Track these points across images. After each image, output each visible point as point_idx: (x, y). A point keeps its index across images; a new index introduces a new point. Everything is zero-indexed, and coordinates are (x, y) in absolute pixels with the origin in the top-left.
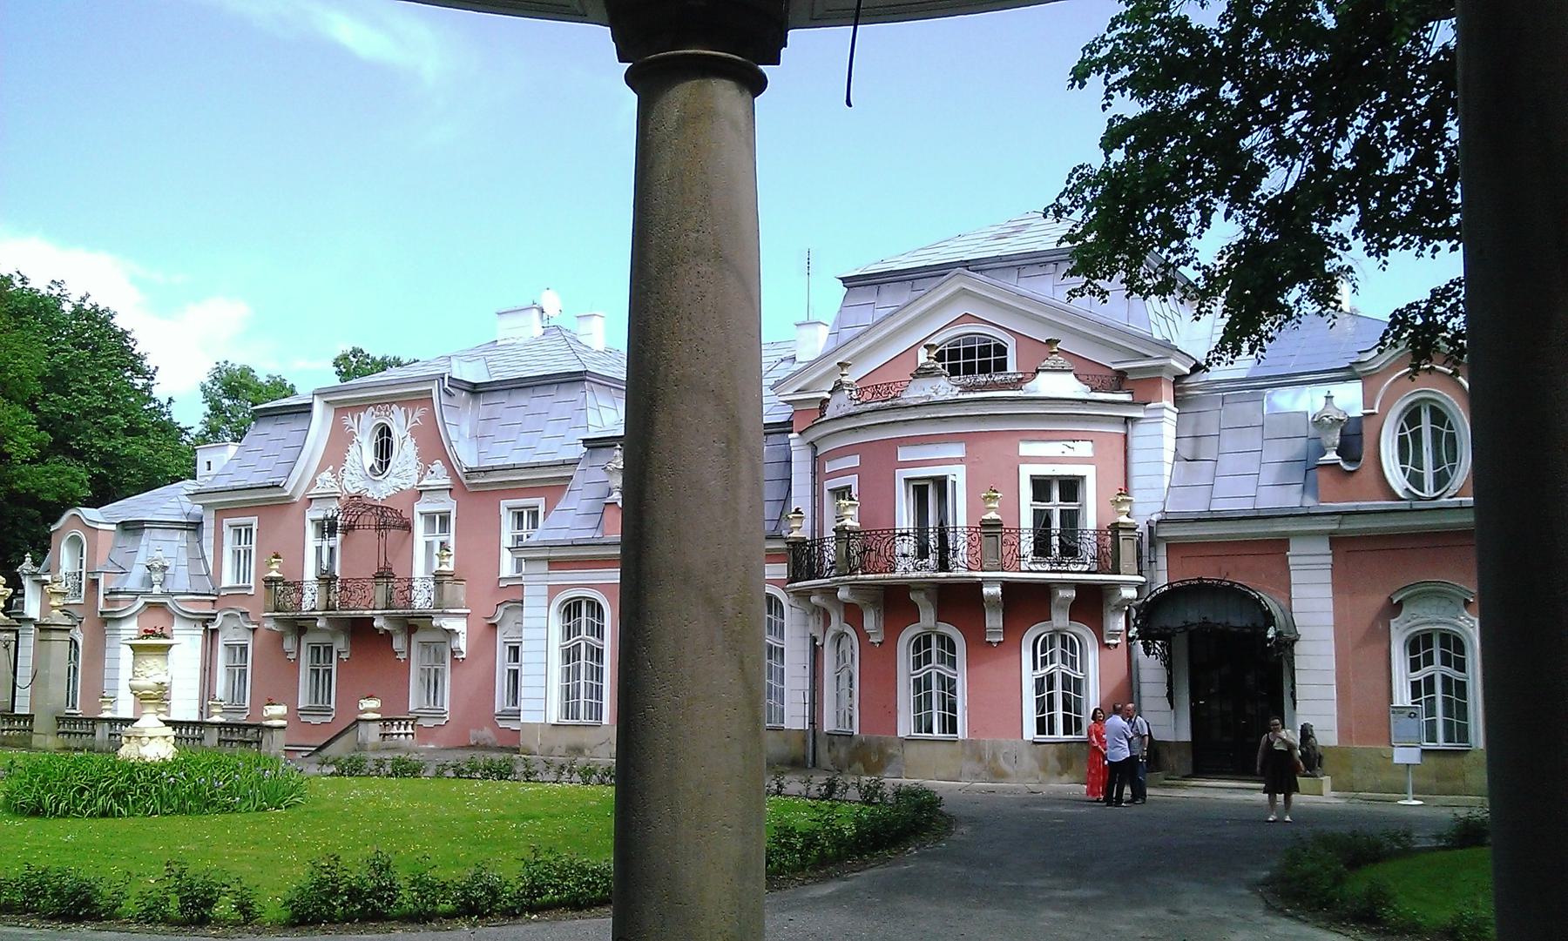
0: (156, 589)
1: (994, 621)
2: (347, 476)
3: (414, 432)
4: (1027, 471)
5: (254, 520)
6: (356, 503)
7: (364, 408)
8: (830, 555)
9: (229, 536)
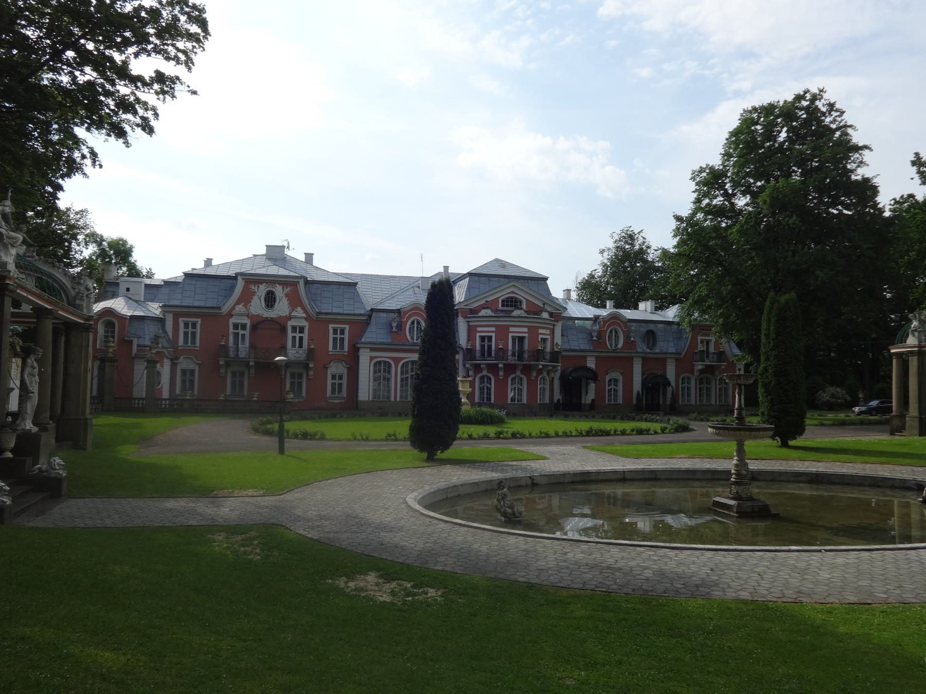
0: (160, 345)
1: (534, 374)
2: (251, 308)
3: (287, 295)
4: (540, 336)
5: (199, 321)
6: (267, 320)
7: (262, 283)
8: (478, 354)
9: (182, 326)
